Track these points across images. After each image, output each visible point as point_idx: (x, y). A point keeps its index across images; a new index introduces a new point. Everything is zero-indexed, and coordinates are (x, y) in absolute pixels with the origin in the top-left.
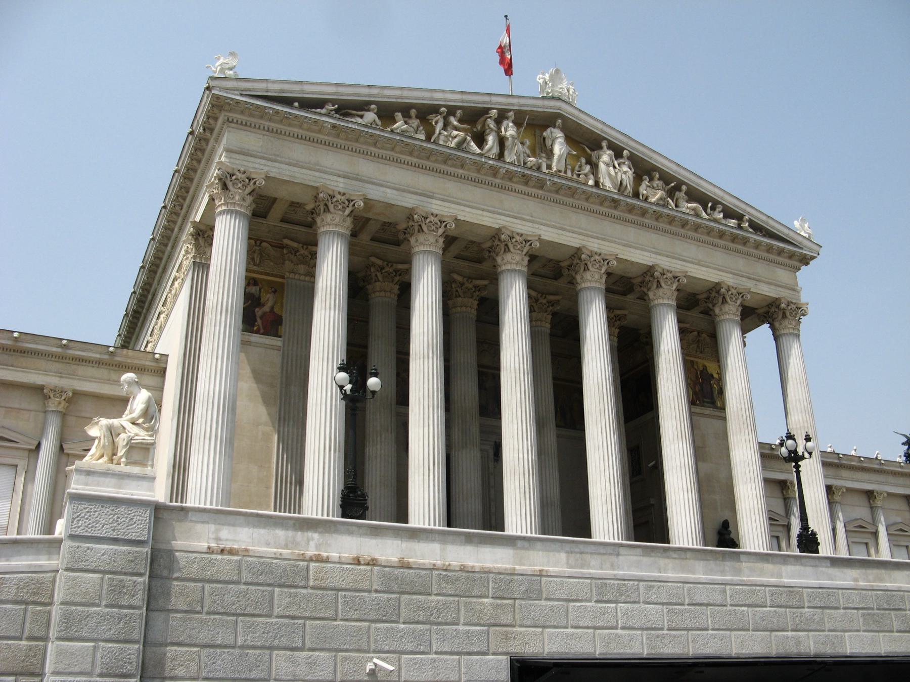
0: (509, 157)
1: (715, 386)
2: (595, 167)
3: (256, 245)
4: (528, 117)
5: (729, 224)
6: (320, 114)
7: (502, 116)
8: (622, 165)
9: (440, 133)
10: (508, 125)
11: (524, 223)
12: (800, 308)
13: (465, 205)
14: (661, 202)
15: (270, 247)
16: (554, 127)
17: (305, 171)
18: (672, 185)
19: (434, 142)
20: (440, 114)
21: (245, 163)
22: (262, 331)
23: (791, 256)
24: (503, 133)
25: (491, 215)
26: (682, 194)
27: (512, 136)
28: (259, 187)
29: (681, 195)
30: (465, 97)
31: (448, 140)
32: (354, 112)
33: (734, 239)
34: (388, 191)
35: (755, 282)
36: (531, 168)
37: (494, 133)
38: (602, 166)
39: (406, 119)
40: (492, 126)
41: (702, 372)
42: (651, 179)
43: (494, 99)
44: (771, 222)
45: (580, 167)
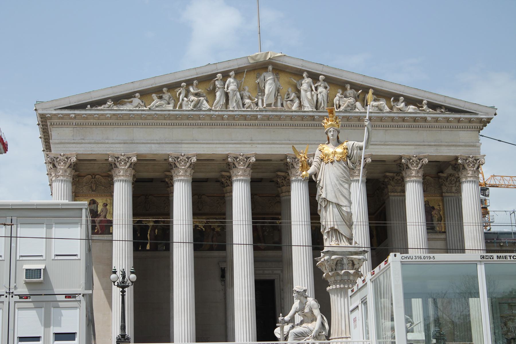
0: (232, 105)
1: (435, 215)
2: (298, 92)
3: (92, 178)
7: (226, 75)
9: (183, 100)
11: (245, 146)
12: (478, 160)
13: (204, 144)
15: (101, 178)
16: (267, 72)
17: (100, 145)
18: (360, 92)
20: (182, 87)
21: (64, 149)
22: (100, 232)
23: (470, 121)
24: (226, 90)
25: (222, 146)
27: (234, 91)
28: (73, 162)
29: (370, 96)
31: (189, 103)
32: (126, 100)
33: (415, 120)
34: (153, 145)
35: (435, 148)
37: (221, 90)
38: (302, 92)
40: (218, 86)
42: (344, 89)
44: (448, 100)
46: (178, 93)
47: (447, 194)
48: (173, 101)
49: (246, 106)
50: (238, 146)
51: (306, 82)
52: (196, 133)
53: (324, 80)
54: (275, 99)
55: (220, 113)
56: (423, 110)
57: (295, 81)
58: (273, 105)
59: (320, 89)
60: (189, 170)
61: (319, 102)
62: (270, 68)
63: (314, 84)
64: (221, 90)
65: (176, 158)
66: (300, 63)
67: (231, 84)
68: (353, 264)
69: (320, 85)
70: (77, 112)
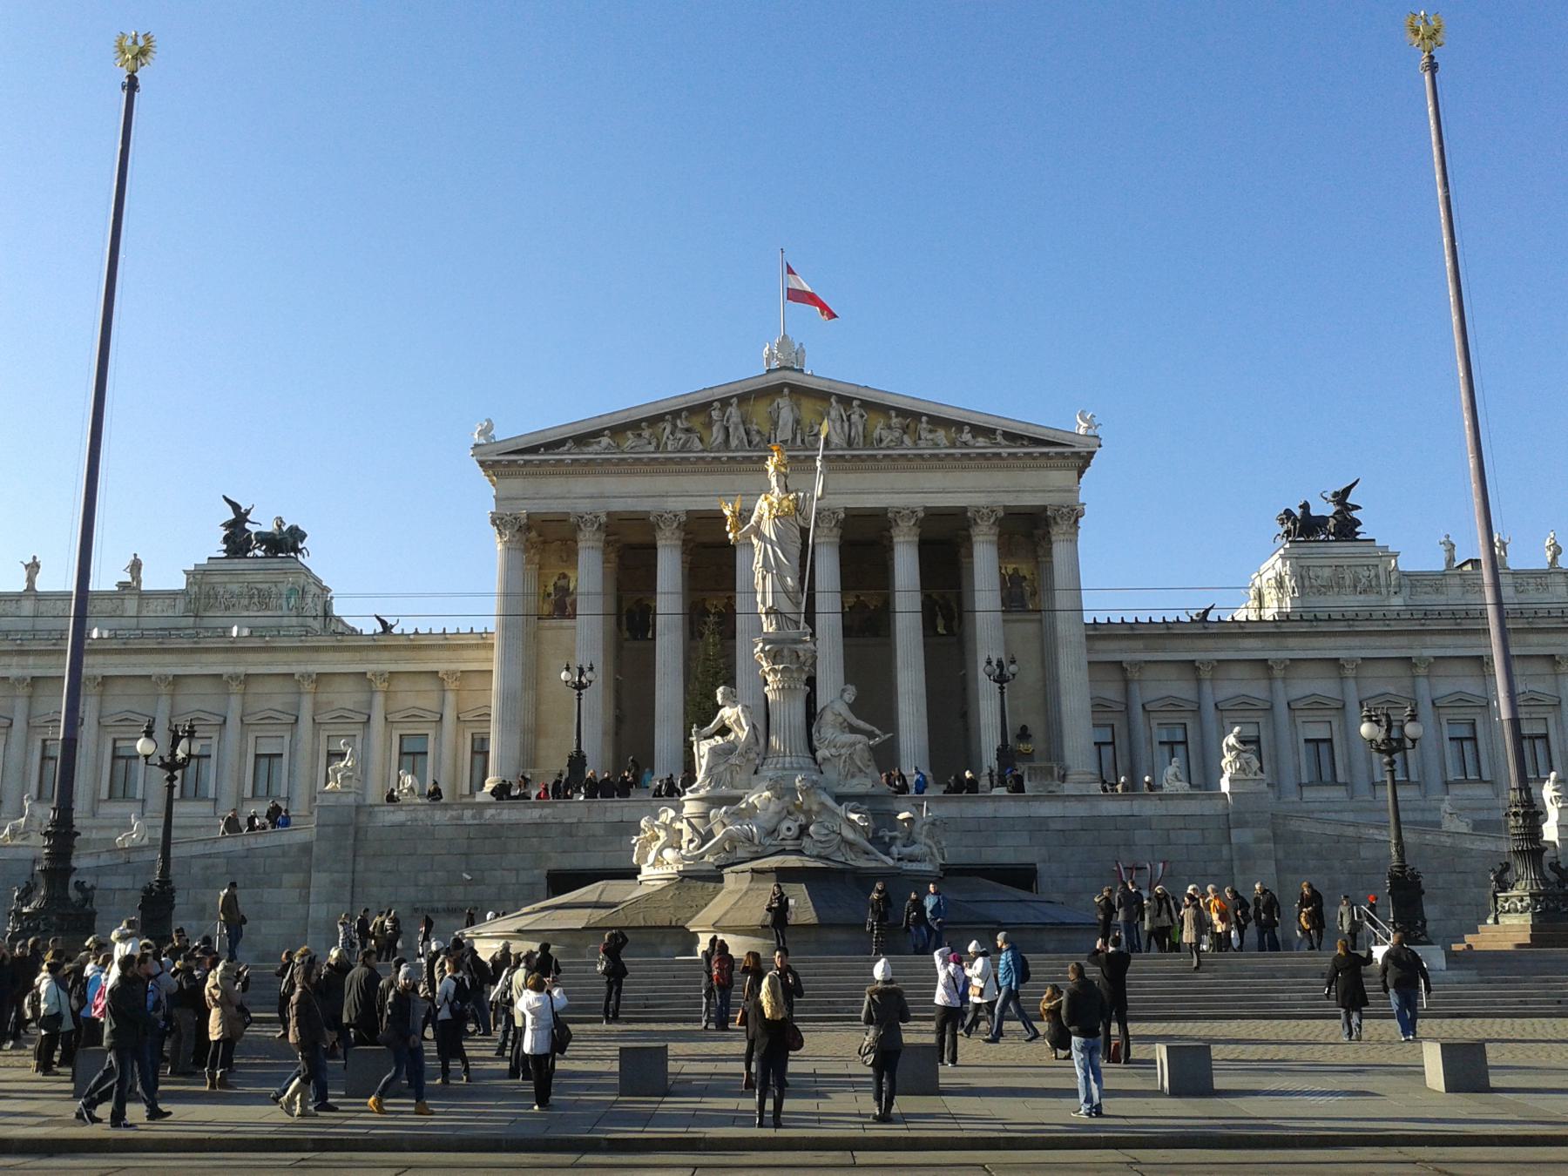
0: (734, 443)
5: (977, 445)
8: (852, 416)
9: (668, 438)
14: (893, 444)
26: (924, 425)
27: (734, 423)
30: (687, 398)
34: (629, 500)
35: (1015, 494)
37: (718, 424)
40: (715, 418)
41: (1010, 577)
42: (890, 418)
44: (1032, 429)
45: (812, 427)
46: (661, 430)
47: (1044, 559)
49: (754, 443)
51: (835, 410)
53: (859, 406)
55: (717, 454)
56: (998, 443)
59: (855, 418)
60: (677, 533)
61: (853, 434)
62: (786, 390)
63: (845, 410)
64: (718, 424)
66: (827, 383)
68: (798, 657)
69: (854, 413)
70: (527, 457)
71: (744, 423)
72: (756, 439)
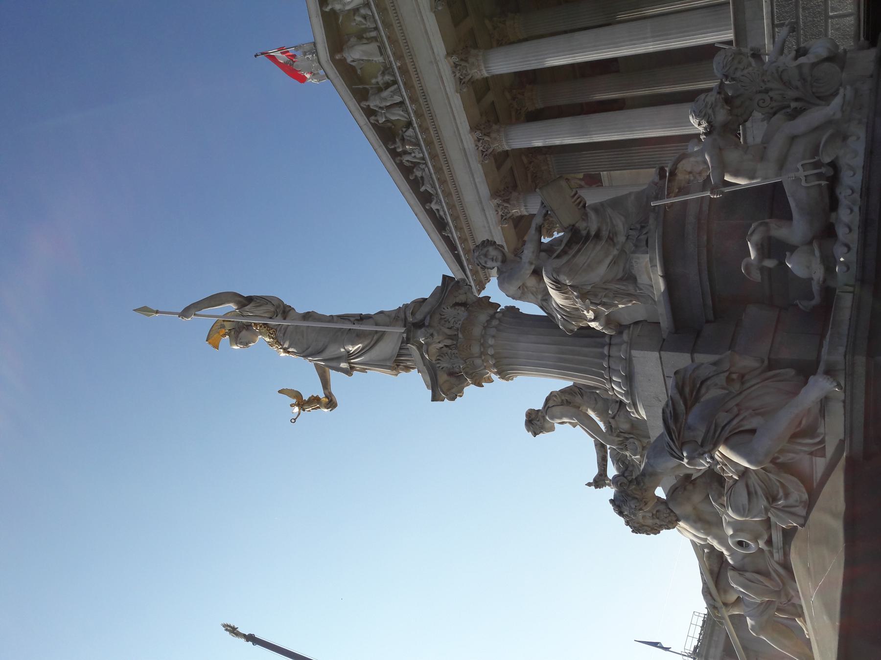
0: (398, 99)
4: (354, 87)
6: (453, 236)
9: (415, 157)
10: (372, 106)
11: (442, 70)
13: (456, 123)
16: (345, 59)
19: (423, 159)
20: (401, 161)
30: (377, 147)
32: (438, 215)
34: (477, 180)
36: (394, 75)
38: (348, 8)
39: (419, 179)
40: (384, 120)
43: (362, 123)
48: (420, 166)
49: (392, 78)
50: (444, 78)
52: (447, 133)
54: (372, 42)
55: (412, 115)
57: (341, 18)
58: (379, 44)
62: (338, 57)
64: (388, 115)
65: (483, 154)
67: (375, 104)
70: (465, 264)
71: (380, 90)
72: (388, 78)
